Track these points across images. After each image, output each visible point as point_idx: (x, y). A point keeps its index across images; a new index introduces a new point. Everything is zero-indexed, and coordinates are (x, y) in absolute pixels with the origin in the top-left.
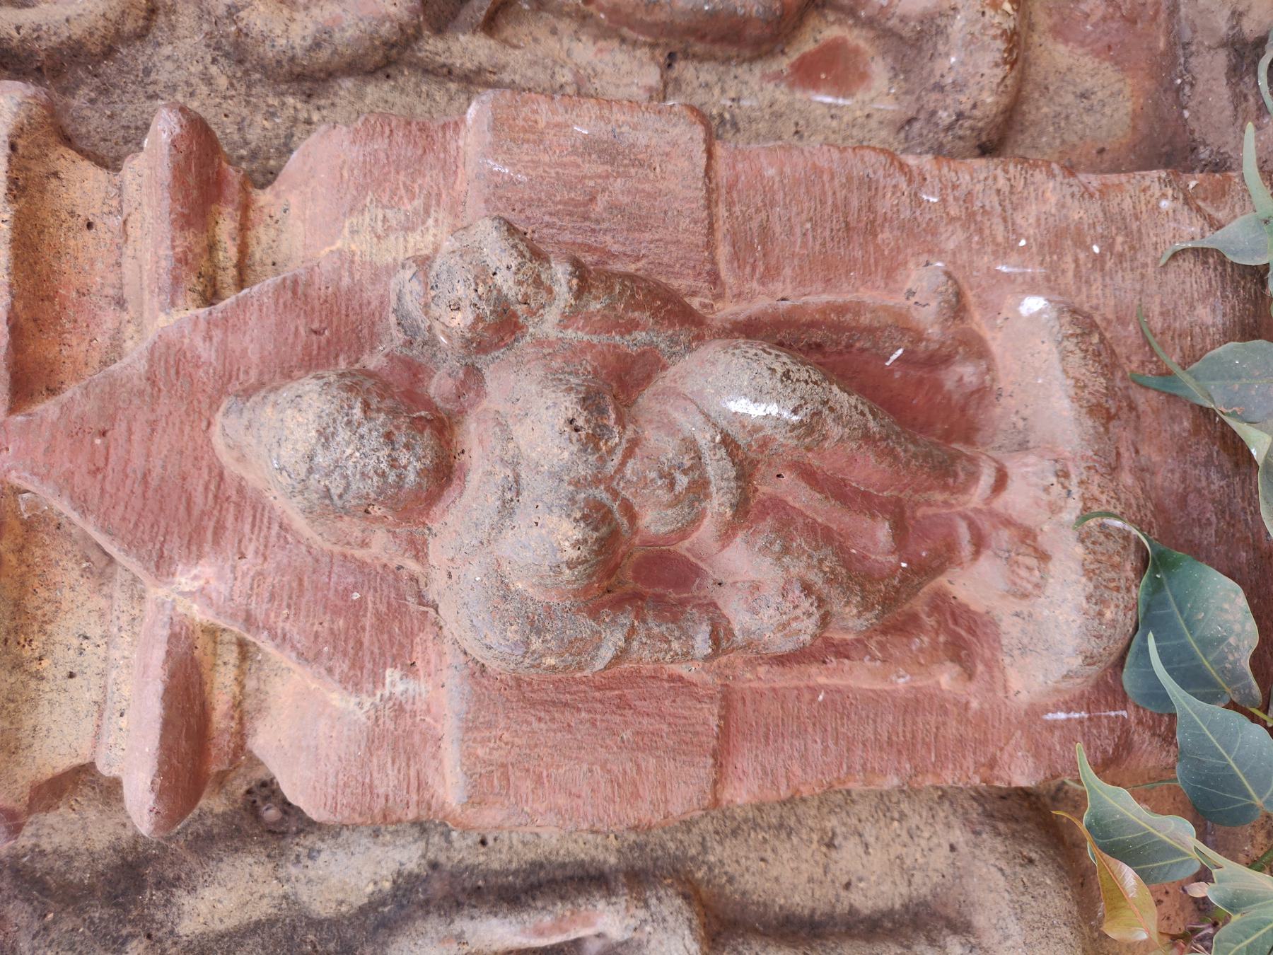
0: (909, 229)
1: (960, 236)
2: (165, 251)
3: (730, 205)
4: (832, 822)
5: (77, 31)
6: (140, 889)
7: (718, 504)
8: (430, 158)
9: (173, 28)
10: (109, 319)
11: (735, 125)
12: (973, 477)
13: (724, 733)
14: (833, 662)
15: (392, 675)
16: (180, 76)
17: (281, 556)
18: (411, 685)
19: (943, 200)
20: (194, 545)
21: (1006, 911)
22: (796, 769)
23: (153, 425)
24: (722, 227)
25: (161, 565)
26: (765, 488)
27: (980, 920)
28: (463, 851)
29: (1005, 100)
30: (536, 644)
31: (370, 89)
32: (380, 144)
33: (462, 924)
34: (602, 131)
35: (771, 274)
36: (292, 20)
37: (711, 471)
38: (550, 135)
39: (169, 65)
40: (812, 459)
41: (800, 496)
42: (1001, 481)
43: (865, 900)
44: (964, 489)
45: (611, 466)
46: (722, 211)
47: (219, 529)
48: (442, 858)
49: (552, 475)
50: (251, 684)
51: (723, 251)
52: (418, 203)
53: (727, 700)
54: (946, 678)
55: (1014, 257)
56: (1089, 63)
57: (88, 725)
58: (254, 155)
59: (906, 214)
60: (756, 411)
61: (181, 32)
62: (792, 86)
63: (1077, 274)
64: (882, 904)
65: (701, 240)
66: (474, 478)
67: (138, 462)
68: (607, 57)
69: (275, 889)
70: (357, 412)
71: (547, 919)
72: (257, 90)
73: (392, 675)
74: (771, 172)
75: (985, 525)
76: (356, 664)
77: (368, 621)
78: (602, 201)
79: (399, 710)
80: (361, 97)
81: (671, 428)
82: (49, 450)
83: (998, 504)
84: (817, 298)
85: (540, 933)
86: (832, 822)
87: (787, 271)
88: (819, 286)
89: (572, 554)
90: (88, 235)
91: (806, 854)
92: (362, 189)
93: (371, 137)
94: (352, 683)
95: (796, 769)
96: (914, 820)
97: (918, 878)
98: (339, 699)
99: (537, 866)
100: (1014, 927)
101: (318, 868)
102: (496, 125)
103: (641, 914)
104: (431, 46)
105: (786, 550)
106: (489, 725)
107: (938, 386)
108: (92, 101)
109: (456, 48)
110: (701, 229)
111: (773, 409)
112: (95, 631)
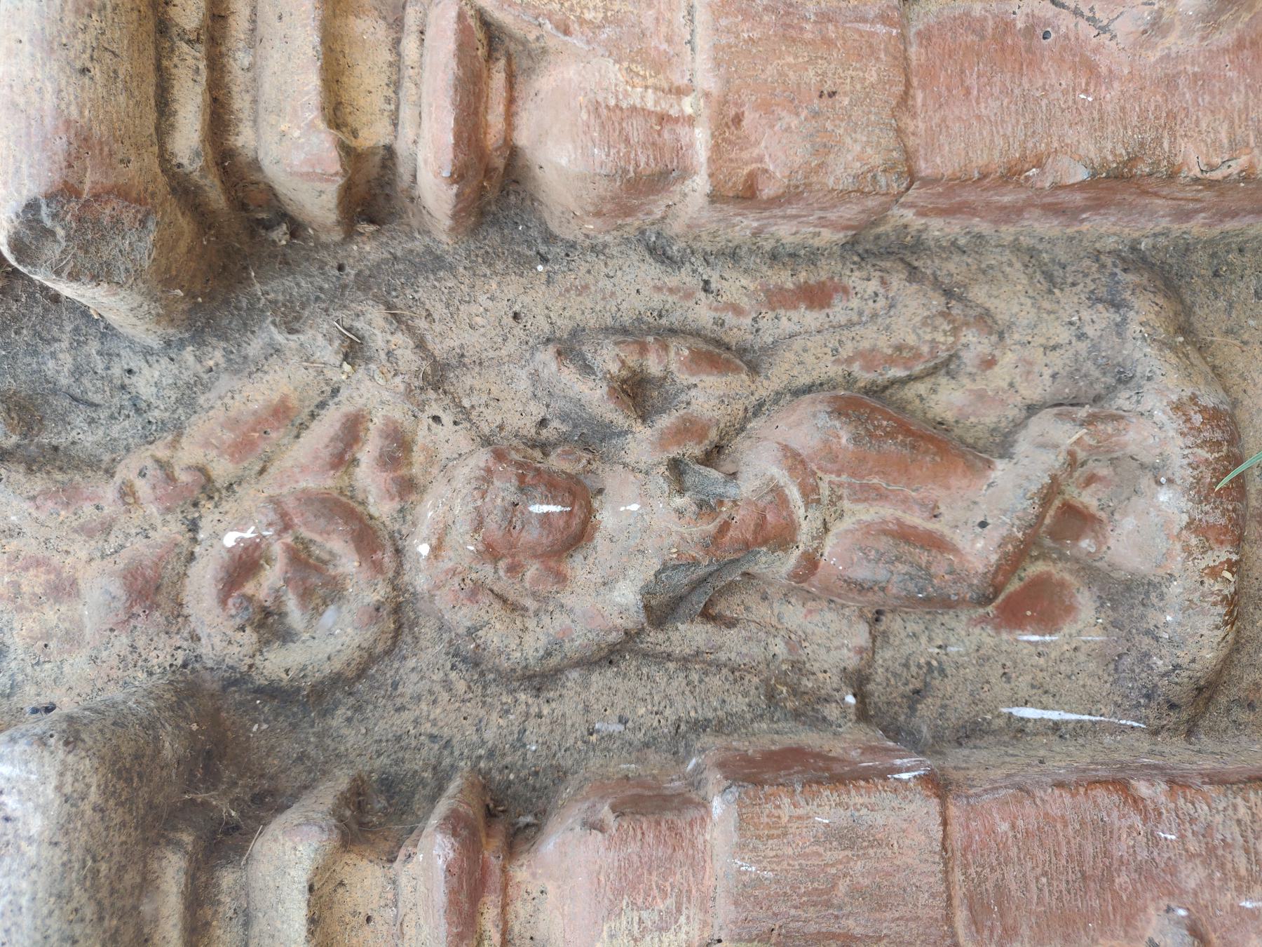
0: (1145, 872)
1: (1201, 873)
3: (966, 866)
5: (337, 665)
8: (680, 855)
11: (942, 672)
16: (424, 686)
19: (1182, 837)
24: (959, 893)
31: (595, 677)
32: (633, 848)
36: (525, 630)
38: (793, 826)
39: (414, 677)
46: (958, 876)
51: (961, 916)
52: (670, 901)
58: (491, 754)
59: (1143, 855)
61: (423, 643)
62: (997, 628)
65: (939, 913)
68: (816, 618)
72: (492, 689)
74: (1004, 827)
78: (842, 887)
80: (586, 686)
87: (1025, 931)
90: (367, 929)
92: (619, 893)
93: (624, 842)
102: (743, 823)
104: (654, 638)
108: (349, 720)
109: (675, 637)
110: (940, 902)
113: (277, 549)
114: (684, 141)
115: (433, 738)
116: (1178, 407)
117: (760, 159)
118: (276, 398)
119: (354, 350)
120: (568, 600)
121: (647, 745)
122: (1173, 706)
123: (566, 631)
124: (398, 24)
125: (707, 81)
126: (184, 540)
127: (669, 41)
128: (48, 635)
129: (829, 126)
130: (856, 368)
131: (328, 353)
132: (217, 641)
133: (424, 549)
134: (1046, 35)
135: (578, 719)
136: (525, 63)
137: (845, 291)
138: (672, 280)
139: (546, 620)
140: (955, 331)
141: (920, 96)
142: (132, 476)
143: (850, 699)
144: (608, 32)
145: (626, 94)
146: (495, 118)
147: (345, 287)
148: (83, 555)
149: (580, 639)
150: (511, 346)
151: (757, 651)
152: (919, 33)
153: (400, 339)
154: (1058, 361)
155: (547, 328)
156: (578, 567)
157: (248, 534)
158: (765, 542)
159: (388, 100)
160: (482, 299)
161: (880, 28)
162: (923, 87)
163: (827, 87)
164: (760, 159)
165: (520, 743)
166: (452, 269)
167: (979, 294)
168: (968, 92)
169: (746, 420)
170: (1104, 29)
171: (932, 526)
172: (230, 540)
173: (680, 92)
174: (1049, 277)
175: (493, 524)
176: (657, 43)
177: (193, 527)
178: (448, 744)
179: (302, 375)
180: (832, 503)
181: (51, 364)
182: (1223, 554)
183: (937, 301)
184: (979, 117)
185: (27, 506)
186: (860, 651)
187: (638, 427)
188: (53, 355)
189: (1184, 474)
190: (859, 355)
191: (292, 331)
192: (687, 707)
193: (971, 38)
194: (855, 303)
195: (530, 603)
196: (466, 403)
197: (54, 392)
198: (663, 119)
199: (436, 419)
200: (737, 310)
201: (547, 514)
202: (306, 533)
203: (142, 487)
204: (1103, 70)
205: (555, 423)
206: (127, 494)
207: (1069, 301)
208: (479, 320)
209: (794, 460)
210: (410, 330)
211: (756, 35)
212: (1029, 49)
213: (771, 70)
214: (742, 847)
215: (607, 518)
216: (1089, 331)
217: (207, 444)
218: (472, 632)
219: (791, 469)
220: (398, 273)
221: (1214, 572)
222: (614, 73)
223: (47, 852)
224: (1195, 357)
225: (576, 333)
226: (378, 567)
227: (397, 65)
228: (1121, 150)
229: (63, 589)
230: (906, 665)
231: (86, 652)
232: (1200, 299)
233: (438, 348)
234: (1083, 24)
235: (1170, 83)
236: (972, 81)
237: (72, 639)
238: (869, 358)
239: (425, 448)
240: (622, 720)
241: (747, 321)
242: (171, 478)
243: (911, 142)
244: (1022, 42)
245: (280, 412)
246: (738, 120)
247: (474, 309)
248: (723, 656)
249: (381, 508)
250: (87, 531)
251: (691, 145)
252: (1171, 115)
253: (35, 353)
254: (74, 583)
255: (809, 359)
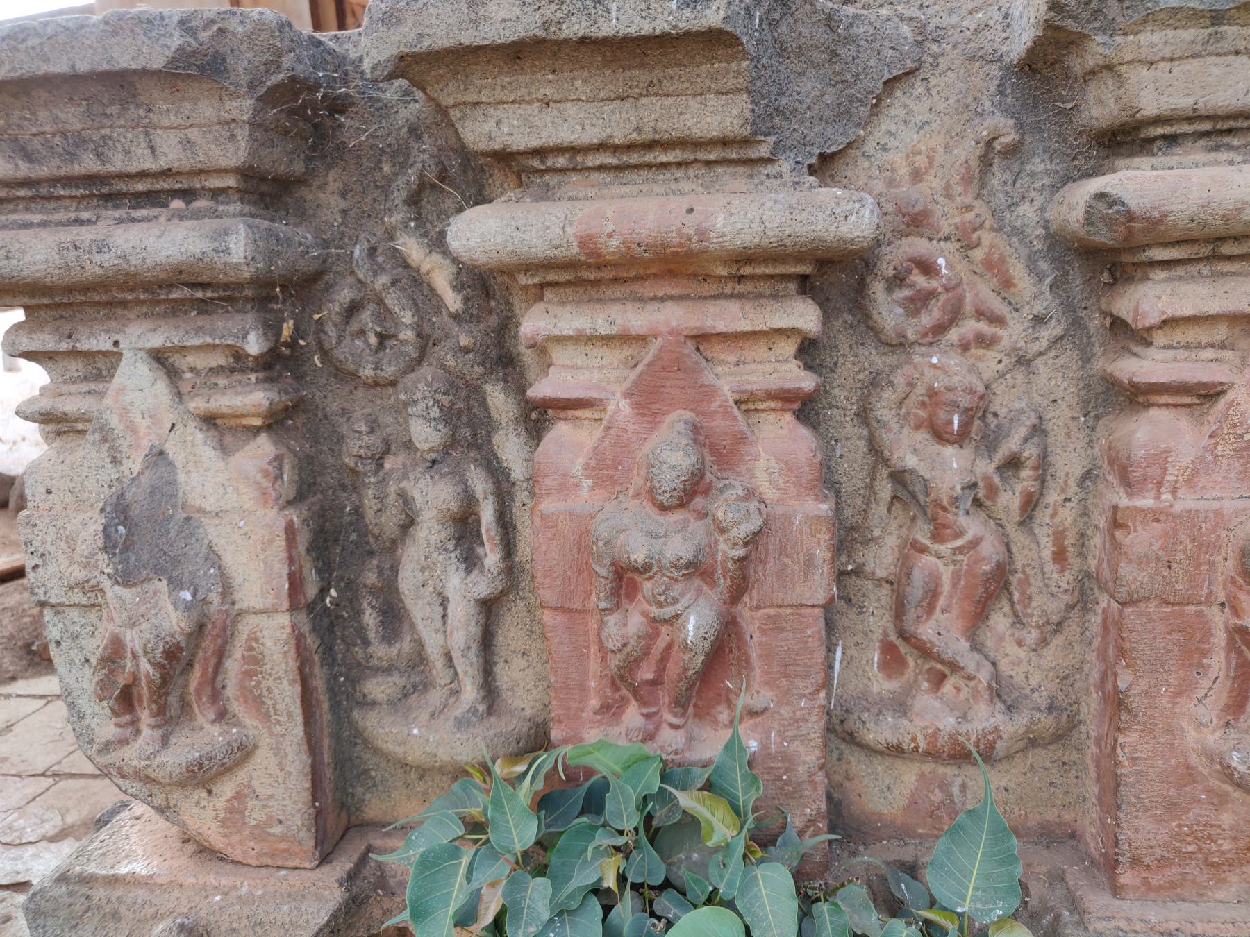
0: (788, 692)
1: (787, 716)
2: (755, 387)
4: (534, 654)
5: (876, 317)
6: (504, 367)
7: (655, 612)
9: (885, 354)
10: (732, 359)
12: (675, 715)
13: (571, 611)
14: (599, 655)
15: (590, 482)
16: (862, 358)
17: (634, 439)
18: (586, 490)
20: (637, 406)
21: (498, 730)
22: (557, 640)
23: (683, 388)
24: (782, 611)
25: (628, 394)
26: (664, 630)
27: (493, 719)
28: (521, 496)
29: (872, 744)
30: (601, 543)
31: (863, 442)
32: (806, 469)
33: (491, 498)
34: (818, 561)
35: (763, 632)
37: (667, 609)
38: (815, 540)
39: (867, 354)
40: (676, 648)
41: (661, 643)
42: (675, 727)
43: (500, 669)
44: (670, 711)
45: (666, 572)
46: (789, 611)
47: (644, 415)
48: (517, 488)
49: (661, 551)
50: (586, 422)
51: (772, 611)
52: (782, 486)
53: (583, 612)
54: (594, 703)
55: (779, 740)
56: (907, 792)
57: (568, 362)
58: (827, 392)
59: (795, 692)
60: (690, 627)
61: (883, 358)
62: (881, 641)
63: (772, 768)
64: (498, 677)
66: (661, 519)
67: (669, 383)
69: (504, 421)
70: (683, 478)
71: (493, 533)
72: (859, 392)
73: (590, 482)
74: (809, 632)
75: (656, 719)
76: (593, 469)
77: (610, 472)
78: (788, 561)
79: (577, 485)
80: (859, 438)
81: (683, 594)
82: (671, 351)
83: (665, 726)
84: (754, 651)
85: (487, 531)
86: (534, 654)
87: (764, 639)
88: (759, 652)
89: (632, 559)
90: (766, 348)
91: (520, 643)
92: (786, 463)
93: (809, 465)
94: (586, 467)
95: (557, 640)
96: (535, 692)
97: (510, 693)
98: (580, 461)
99: (514, 527)
100: (492, 732)
101: (513, 437)
102: (818, 518)
103: (495, 573)
104: (884, 472)
105: (639, 637)
106: (571, 521)
107: (718, 703)
109: (884, 483)
110: (779, 602)
111: (691, 633)
112: (604, 362)
113: (934, 284)
114: (1147, 495)
115: (836, 364)
116: (997, 729)
117: (1135, 531)
118: (1016, 281)
119: (1039, 320)
120: (906, 431)
121: (829, 468)
122: (842, 722)
123: (890, 430)
124: (1223, 346)
125: (1178, 507)
126: (941, 235)
127: (1204, 488)
128: (893, 170)
129: (1152, 565)
130: (1020, 575)
131: (1038, 308)
132: (889, 257)
133: (935, 360)
134: (1198, 673)
135: (843, 434)
136: (1197, 413)
137: (1062, 571)
138: (1071, 482)
139: (895, 420)
140: (1038, 627)
141: (1168, 610)
142: (976, 211)
143: (850, 567)
144: (1210, 458)
145: (1173, 466)
146: (1165, 399)
147: (1075, 311)
148: (934, 185)
149: (886, 437)
150: (1038, 399)
151: (875, 522)
152: (1202, 611)
153: (1045, 343)
154: (1019, 679)
155: (1048, 417)
156: (923, 436)
157: (944, 271)
158: (936, 528)
159: (1178, 343)
160: (1065, 384)
161: (1205, 591)
162: (1172, 612)
163: (1174, 565)
164: (1135, 531)
165: (831, 406)
166: (1083, 367)
167: (1059, 640)
168: (1169, 633)
169: (994, 519)
170: (1200, 701)
171: (938, 609)
172: (941, 261)
173: (1174, 492)
174: (1066, 677)
175: (950, 396)
176: (1202, 481)
177: (947, 239)
178: (833, 371)
179: (1027, 295)
180: (953, 561)
181: (1038, 160)
182: (923, 745)
183: (1055, 618)
184: (1155, 638)
185: (963, 159)
186: (873, 573)
187: (994, 465)
188: (1043, 161)
189: (964, 728)
190: (1027, 577)
191: (1051, 287)
192: (847, 488)
193: (1198, 636)
194: (1055, 576)
195: (903, 411)
196: (1008, 376)
197: (1022, 163)
198: (1160, 484)
199: (1000, 361)
200: (1053, 516)
201: (952, 423)
202: (943, 298)
203: (970, 216)
204: (1178, 700)
205: (995, 422)
206: (968, 208)
207: (1053, 686)
208: (1053, 383)
209: (975, 543)
210: (1049, 348)
211: (1204, 530)
212: (1190, 664)
213: (1184, 538)
214: (807, 517)
215: (949, 450)
216: (1036, 695)
217: (991, 247)
218: (891, 383)
219: (970, 542)
220: (1081, 339)
221: (914, 739)
222: (1186, 460)
223: (832, 235)
224: (1021, 744)
225: (1044, 432)
226: (925, 335)
227: (1199, 347)
228: (1134, 705)
229: (917, 176)
230: (864, 595)
231: (885, 190)
232: (1051, 754)
233: (1039, 362)
234: (1204, 691)
235: (1169, 731)
236: (1175, 636)
237: (891, 183)
238: (1026, 581)
239: (984, 355)
240: (841, 456)
241: (1047, 520)
242: (975, 230)
243: (1142, 605)
244: (1195, 662)
245: (1007, 283)
246: (1157, 520)
247: (1060, 380)
248: (873, 505)
249: (953, 335)
250: (947, 187)
251: (1144, 498)
252: (1152, 731)
253: (1044, 152)
254: (920, 181)
255: (1026, 552)
